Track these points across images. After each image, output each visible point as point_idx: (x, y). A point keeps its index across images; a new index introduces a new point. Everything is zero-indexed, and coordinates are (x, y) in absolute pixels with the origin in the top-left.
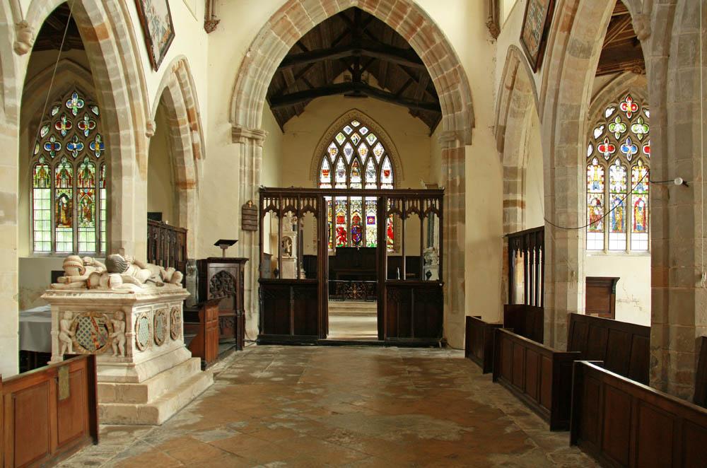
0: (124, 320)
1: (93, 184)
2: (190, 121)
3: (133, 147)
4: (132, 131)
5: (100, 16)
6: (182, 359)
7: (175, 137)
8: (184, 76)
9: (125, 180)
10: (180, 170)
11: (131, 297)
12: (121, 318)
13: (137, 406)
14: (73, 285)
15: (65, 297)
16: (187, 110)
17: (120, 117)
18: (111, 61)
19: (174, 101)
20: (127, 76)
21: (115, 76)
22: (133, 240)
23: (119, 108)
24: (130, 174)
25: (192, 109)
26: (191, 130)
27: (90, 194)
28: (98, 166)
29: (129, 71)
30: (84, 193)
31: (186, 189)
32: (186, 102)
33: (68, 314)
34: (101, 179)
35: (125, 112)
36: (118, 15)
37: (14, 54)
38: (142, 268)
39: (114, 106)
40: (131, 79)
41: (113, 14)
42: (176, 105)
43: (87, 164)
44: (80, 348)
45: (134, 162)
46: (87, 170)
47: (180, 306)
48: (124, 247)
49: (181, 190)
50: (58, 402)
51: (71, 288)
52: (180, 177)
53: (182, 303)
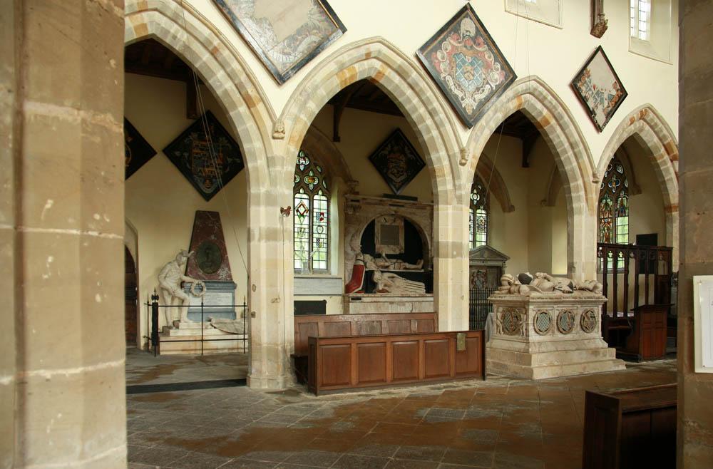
0: (526, 313)
1: (611, 214)
2: (668, 154)
3: (582, 193)
4: (580, 182)
5: (541, 113)
6: (593, 346)
7: (656, 169)
8: (652, 120)
9: (576, 218)
10: (665, 197)
11: (527, 299)
12: (524, 312)
13: (523, 367)
14: (503, 292)
15: (498, 299)
16: (664, 145)
17: (569, 174)
18: (556, 139)
19: (647, 142)
20: (571, 144)
21: (561, 147)
22: (583, 260)
23: (567, 168)
24: (580, 213)
25: (669, 143)
26: (672, 161)
27: (609, 223)
28: (614, 199)
29: (572, 140)
30: (605, 222)
31: (671, 212)
32: (660, 139)
33: (501, 309)
34: (616, 210)
35: (573, 170)
36: (554, 107)
37: (460, 166)
38: (549, 281)
39: (564, 168)
40: (574, 146)
41: (551, 108)
42: (649, 145)
43: (606, 199)
44: (505, 330)
45: (584, 204)
46: (607, 204)
47: (598, 312)
48: (575, 266)
49: (668, 214)
50: (457, 352)
51: (502, 294)
52: (666, 203)
53: (600, 307)
